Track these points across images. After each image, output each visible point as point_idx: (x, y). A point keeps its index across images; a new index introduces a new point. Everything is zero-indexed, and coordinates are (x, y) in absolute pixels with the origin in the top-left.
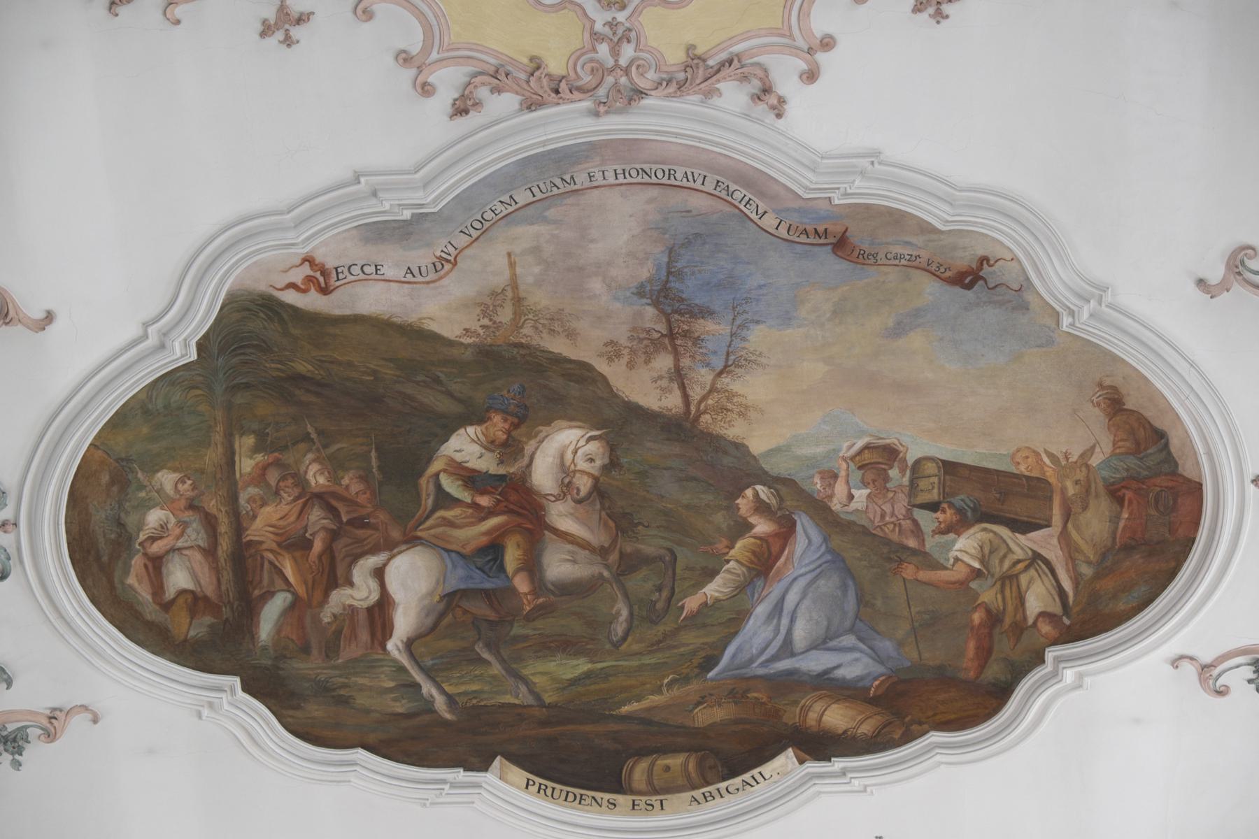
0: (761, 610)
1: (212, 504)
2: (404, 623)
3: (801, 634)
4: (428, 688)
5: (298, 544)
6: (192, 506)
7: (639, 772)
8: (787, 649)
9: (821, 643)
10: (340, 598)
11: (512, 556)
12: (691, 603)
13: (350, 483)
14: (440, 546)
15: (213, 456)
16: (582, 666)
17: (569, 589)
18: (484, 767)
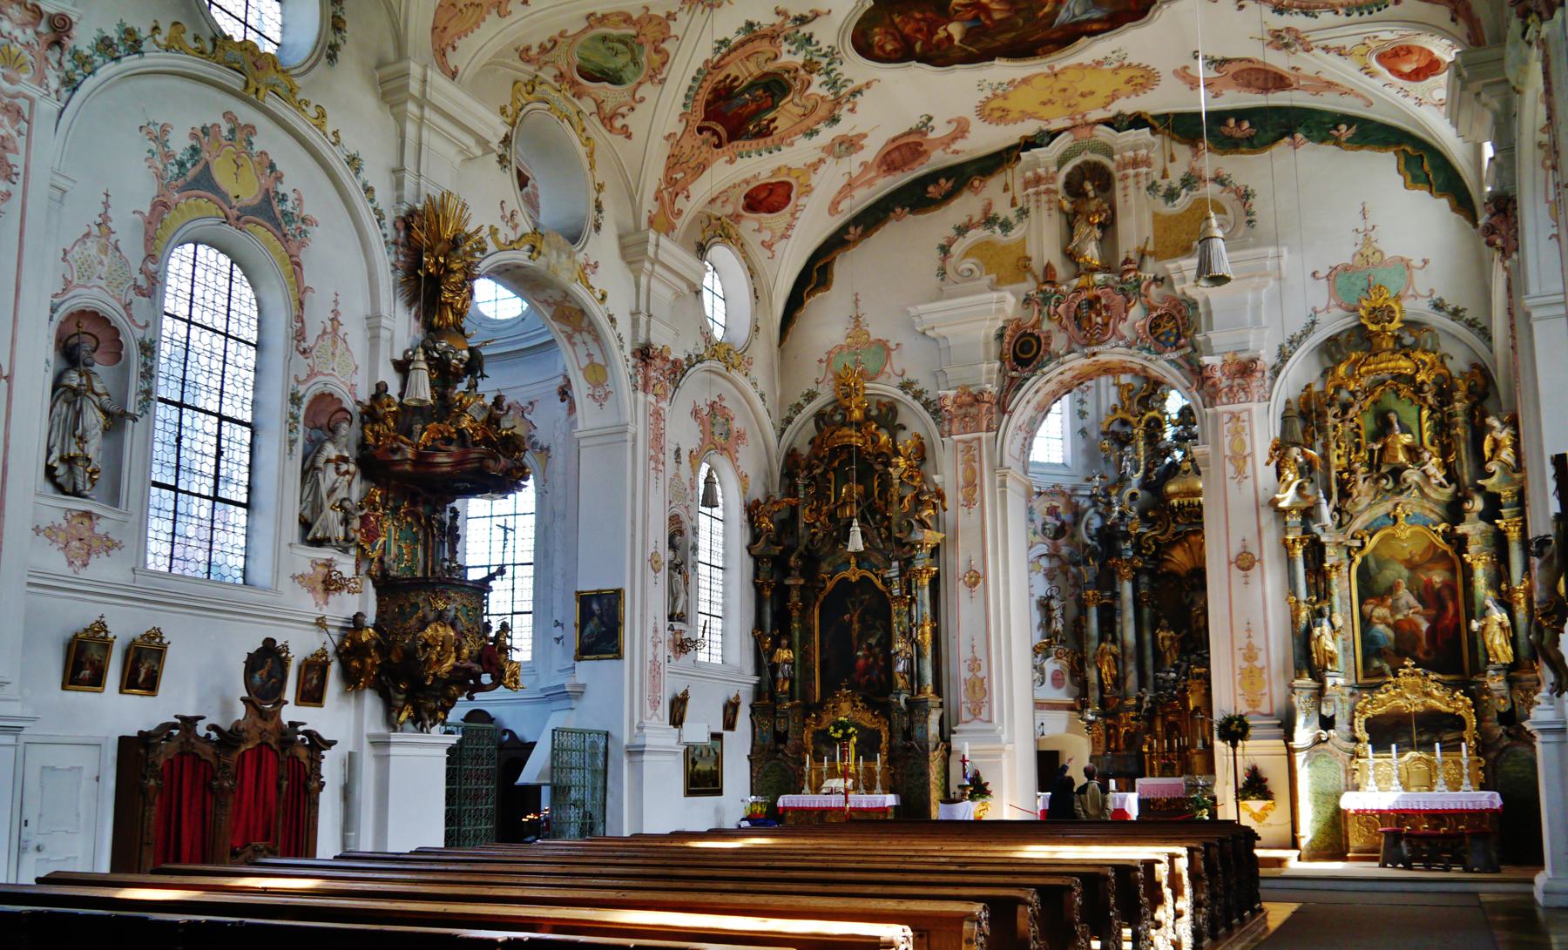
0: (1063, 11)
1: (891, 31)
2: (957, 38)
3: (1077, 11)
4: (970, 49)
5: (919, 30)
6: (886, 33)
7: (1040, 51)
8: (1074, 16)
9: (1086, 12)
10: (936, 38)
11: (983, 17)
12: (1041, 14)
13: (929, 15)
14: (961, 20)
15: (887, 21)
16: (1013, 34)
17: (1001, 20)
18: (993, 59)
